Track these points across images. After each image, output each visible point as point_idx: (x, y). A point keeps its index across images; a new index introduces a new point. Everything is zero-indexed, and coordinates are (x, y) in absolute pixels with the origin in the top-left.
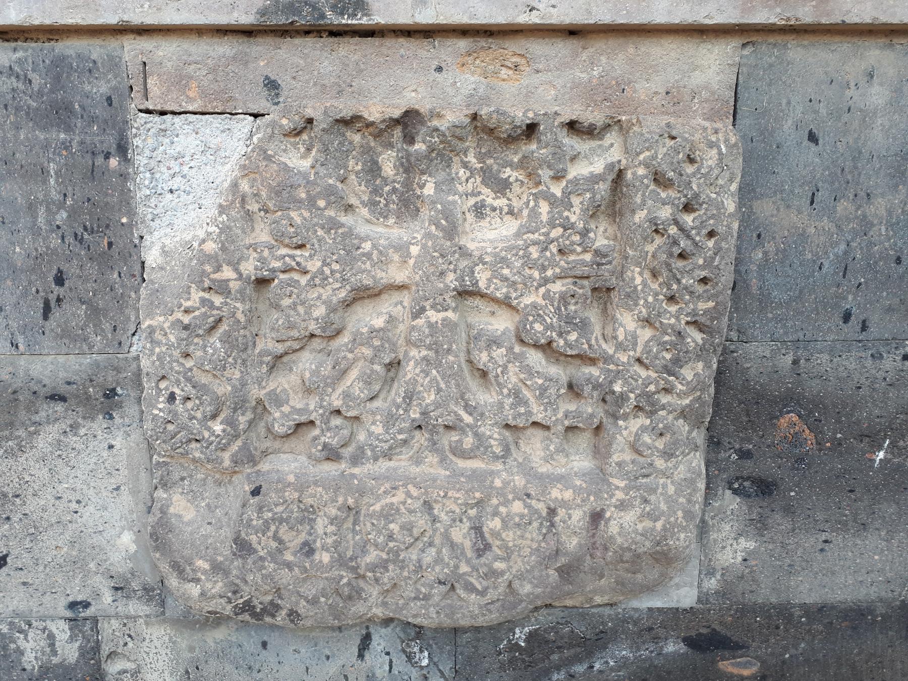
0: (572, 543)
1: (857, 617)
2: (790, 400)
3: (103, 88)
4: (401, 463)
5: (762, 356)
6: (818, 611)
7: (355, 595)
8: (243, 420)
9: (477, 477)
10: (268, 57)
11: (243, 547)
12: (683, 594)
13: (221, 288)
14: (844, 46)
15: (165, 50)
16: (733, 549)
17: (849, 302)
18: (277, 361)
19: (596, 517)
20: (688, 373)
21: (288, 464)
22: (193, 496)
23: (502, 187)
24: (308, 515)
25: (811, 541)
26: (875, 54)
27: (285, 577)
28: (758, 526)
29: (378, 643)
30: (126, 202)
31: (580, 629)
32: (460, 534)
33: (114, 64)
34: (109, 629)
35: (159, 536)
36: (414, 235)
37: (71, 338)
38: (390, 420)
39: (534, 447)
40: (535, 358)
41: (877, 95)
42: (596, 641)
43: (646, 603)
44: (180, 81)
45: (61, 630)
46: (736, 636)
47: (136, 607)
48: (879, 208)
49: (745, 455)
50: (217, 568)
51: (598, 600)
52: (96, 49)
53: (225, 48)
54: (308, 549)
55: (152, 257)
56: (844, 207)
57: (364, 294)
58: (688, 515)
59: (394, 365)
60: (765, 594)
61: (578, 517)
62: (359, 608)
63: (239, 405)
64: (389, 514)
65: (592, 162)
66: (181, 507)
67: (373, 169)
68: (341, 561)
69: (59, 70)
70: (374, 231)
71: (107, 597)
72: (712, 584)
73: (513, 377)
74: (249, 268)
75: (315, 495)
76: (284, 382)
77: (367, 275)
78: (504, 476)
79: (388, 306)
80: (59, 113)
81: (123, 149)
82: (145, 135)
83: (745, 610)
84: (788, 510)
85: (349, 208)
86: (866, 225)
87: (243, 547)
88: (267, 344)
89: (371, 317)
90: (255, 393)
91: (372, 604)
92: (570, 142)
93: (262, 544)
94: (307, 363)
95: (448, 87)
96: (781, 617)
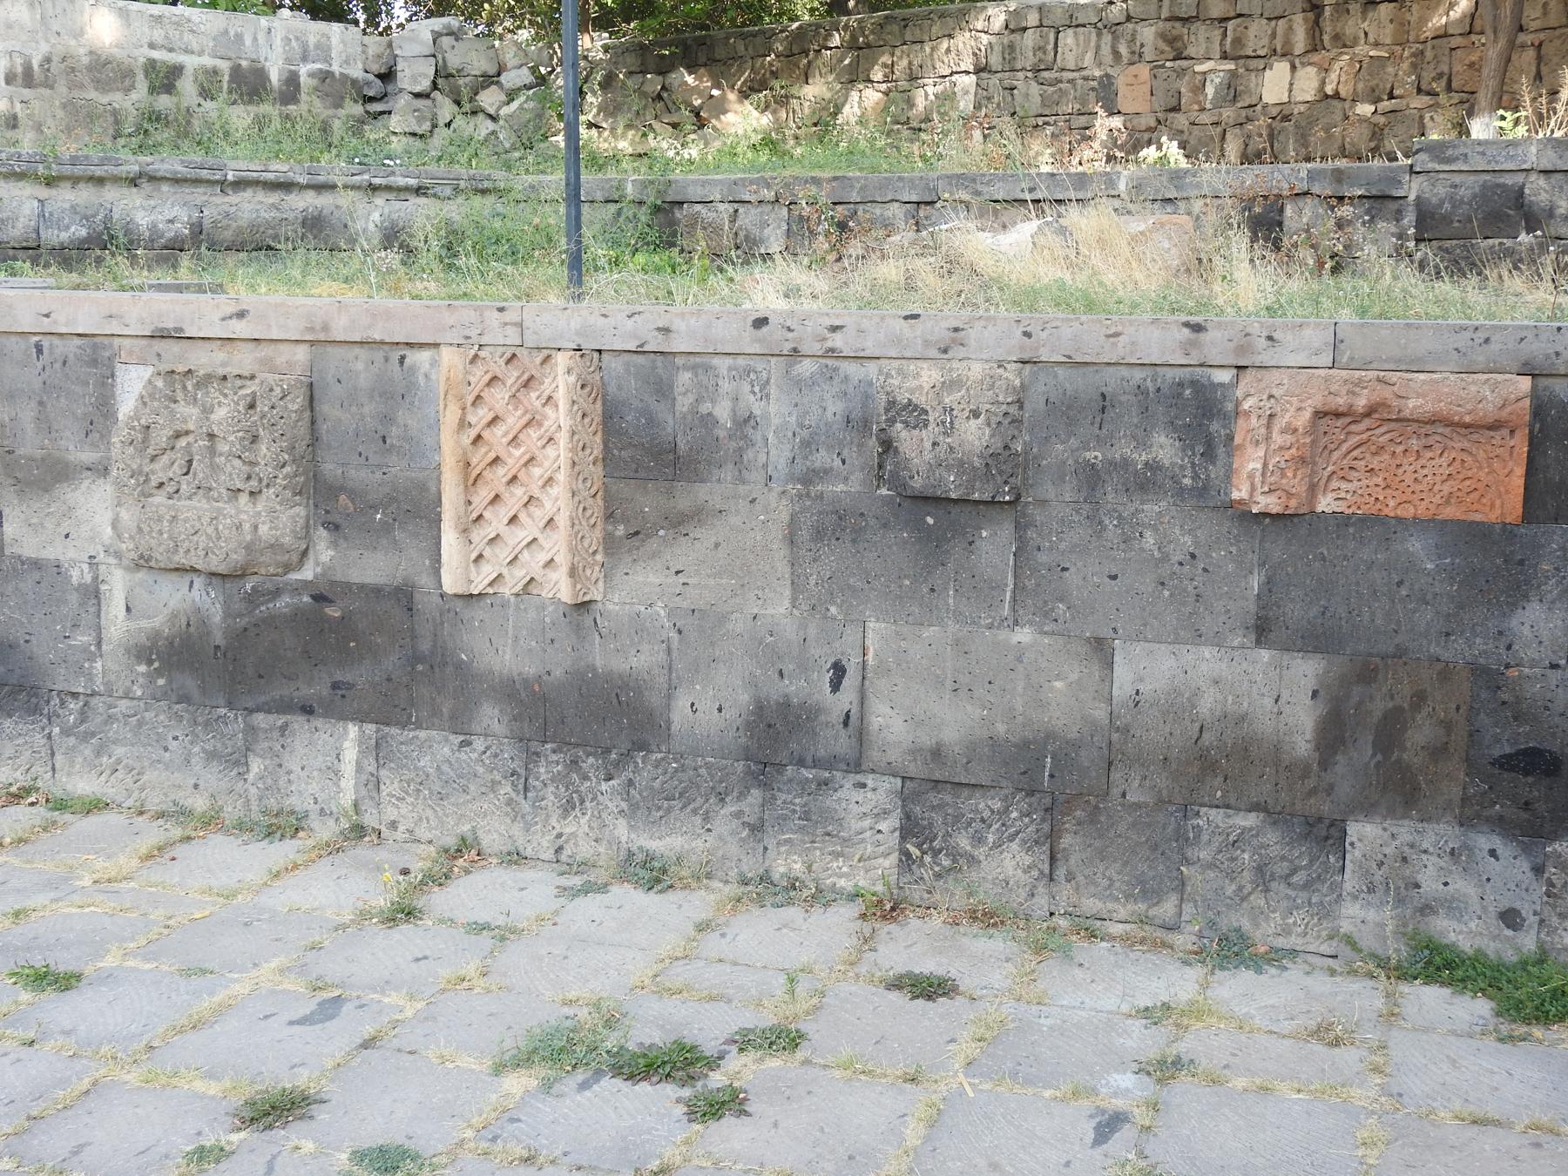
0: (248, 538)
1: (376, 591)
2: (342, 489)
3: (107, 354)
4: (194, 503)
5: (330, 469)
6: (362, 587)
7: (176, 552)
8: (142, 479)
9: (219, 510)
10: (159, 345)
11: (140, 530)
12: (307, 573)
13: (133, 428)
14: (346, 347)
15: (127, 342)
16: (324, 553)
17: (360, 449)
18: (153, 459)
19: (256, 527)
20: (285, 471)
21: (159, 499)
22: (128, 510)
23: (225, 396)
24: (160, 519)
25: (356, 553)
26: (357, 350)
27: (153, 543)
28: (334, 544)
29: (196, 585)
30: (113, 396)
31: (269, 586)
32: (210, 530)
33: (111, 345)
34: (102, 568)
35: (115, 524)
36: (194, 412)
37: (94, 446)
38: (189, 483)
39: (244, 498)
40: (237, 462)
41: (360, 366)
42: (277, 593)
43: (294, 576)
44: (130, 353)
45: (85, 567)
46: (330, 596)
47: (112, 560)
48: (366, 410)
49: (327, 512)
50: (131, 537)
51: (272, 570)
52: (106, 341)
53: (144, 342)
54: (161, 533)
55: (121, 416)
56: (354, 408)
57: (178, 435)
58: (293, 531)
59: (190, 462)
60: (339, 577)
61: (247, 526)
62: (176, 558)
63: (140, 473)
64: (186, 520)
65: (251, 387)
66: (125, 515)
67: (184, 388)
68: (170, 538)
69: (95, 347)
70: (183, 409)
71: (102, 555)
72: (319, 570)
73: (229, 469)
74: (143, 421)
75: (163, 510)
76: (157, 466)
77: (179, 426)
78: (229, 509)
79: (190, 438)
80: (94, 362)
81: (113, 376)
82: (120, 370)
83: (333, 583)
84: (346, 539)
85: (176, 402)
86: (363, 418)
87: (140, 530)
88: (150, 451)
89: (183, 442)
90: (146, 469)
91: (180, 559)
92: (239, 382)
93: (146, 529)
94: (165, 459)
95: (204, 360)
96: (348, 586)
